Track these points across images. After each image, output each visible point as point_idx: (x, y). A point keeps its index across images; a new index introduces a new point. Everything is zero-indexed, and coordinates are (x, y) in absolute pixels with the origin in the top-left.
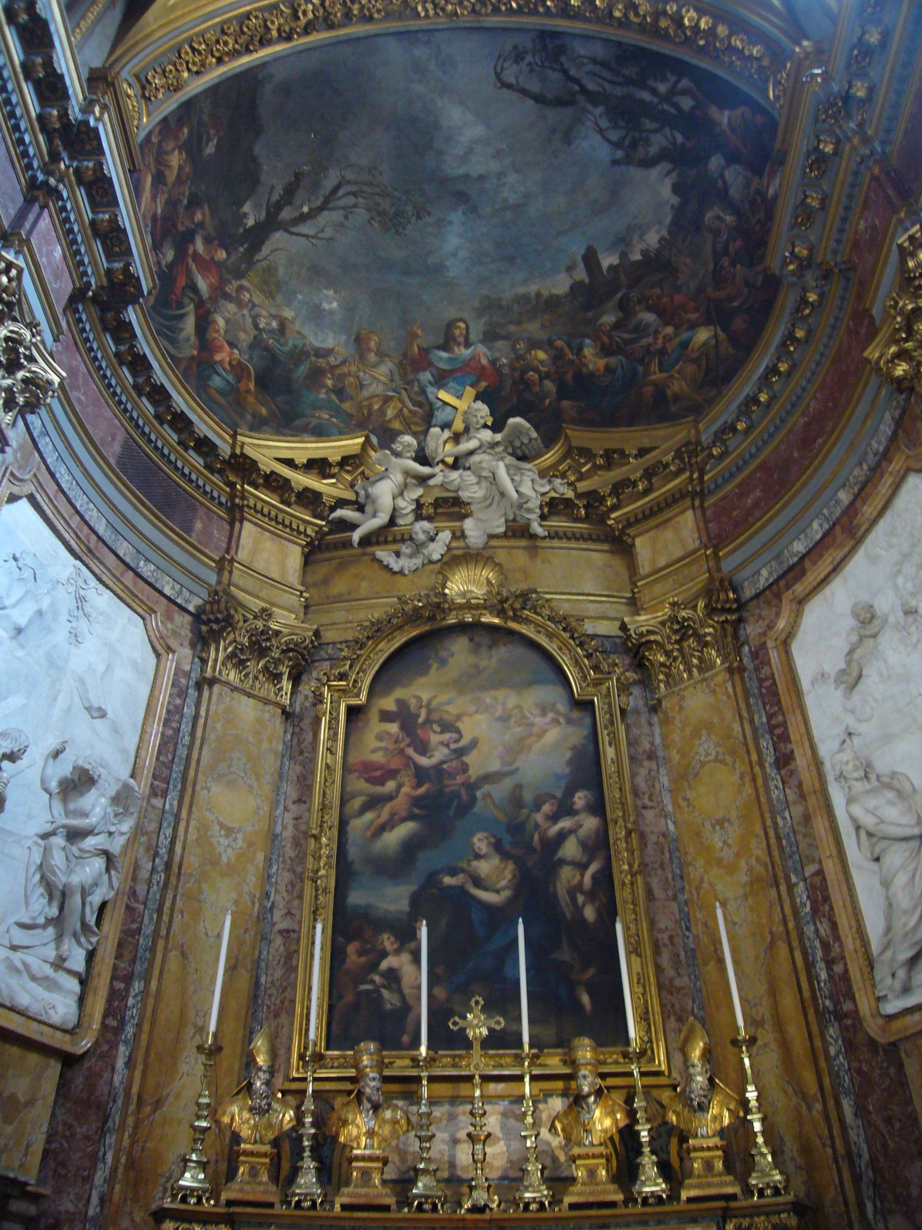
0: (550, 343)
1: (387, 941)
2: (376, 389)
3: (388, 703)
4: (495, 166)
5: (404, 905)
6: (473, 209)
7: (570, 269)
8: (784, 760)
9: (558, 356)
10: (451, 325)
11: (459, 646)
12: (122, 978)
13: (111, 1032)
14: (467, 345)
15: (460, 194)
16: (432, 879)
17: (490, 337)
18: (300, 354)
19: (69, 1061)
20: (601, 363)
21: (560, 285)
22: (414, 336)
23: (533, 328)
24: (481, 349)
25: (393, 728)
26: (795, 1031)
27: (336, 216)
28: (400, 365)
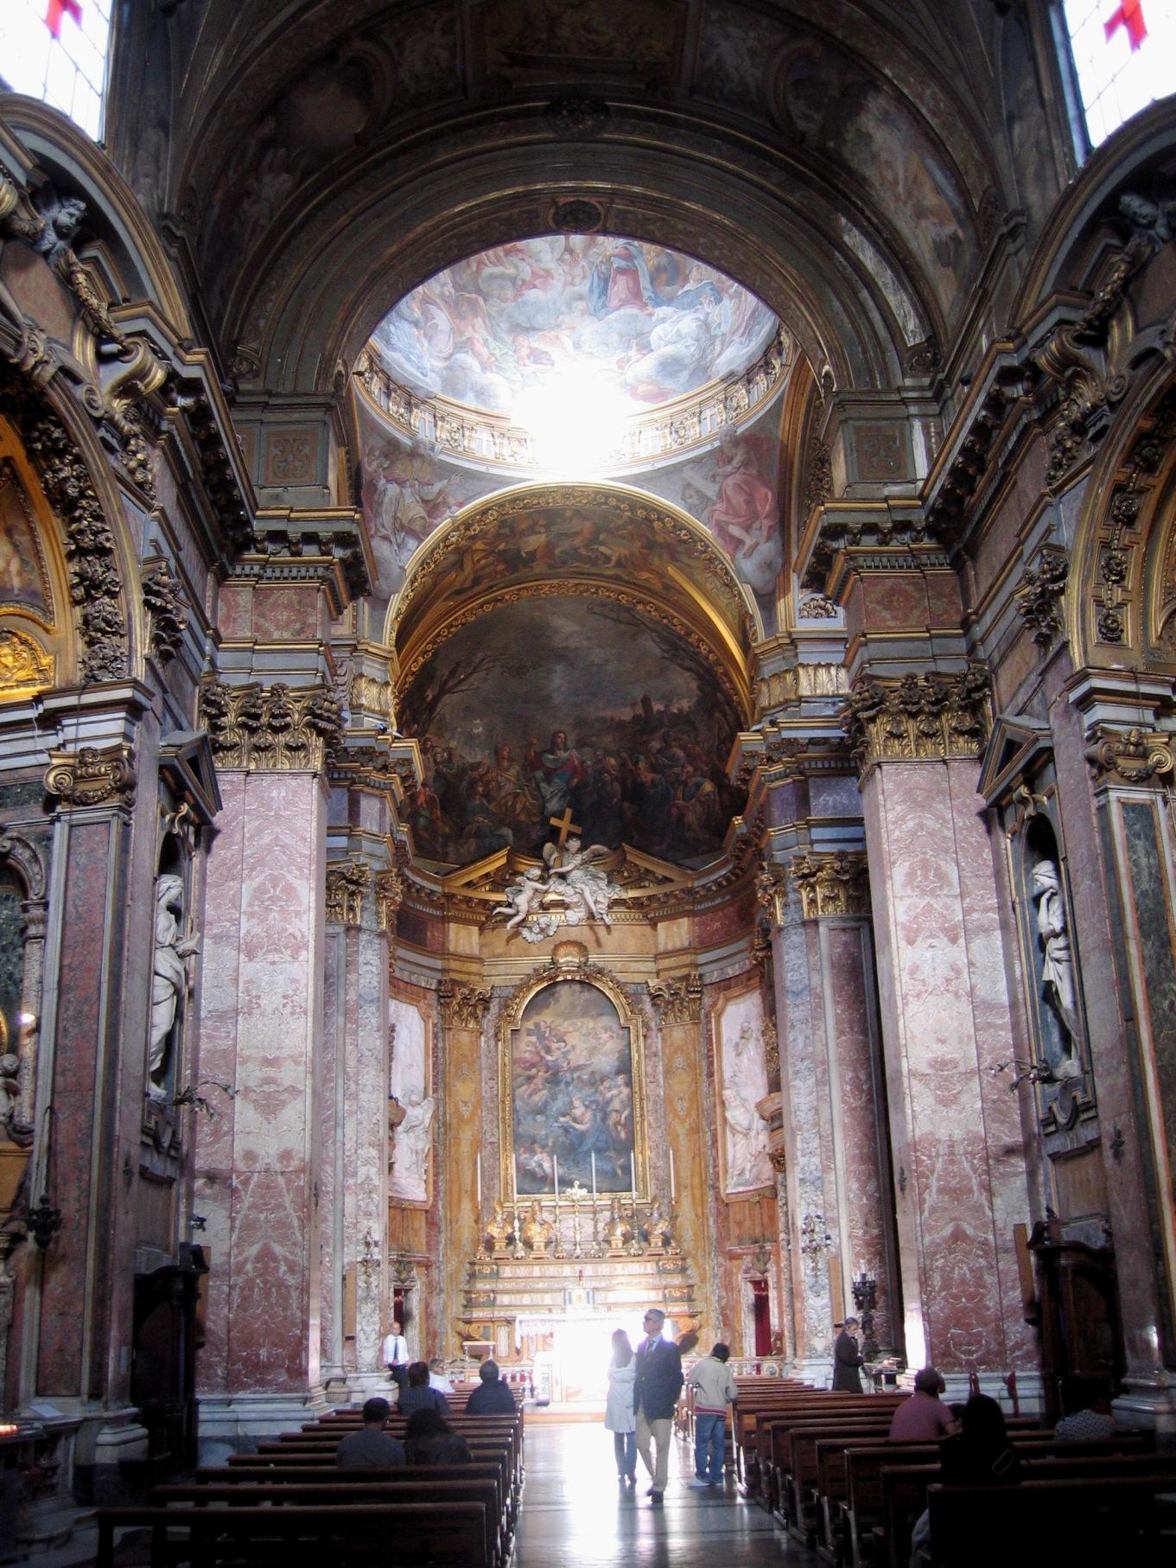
0: (618, 753)
2: (509, 788)
3: (530, 1025)
4: (585, 644)
6: (572, 664)
7: (633, 705)
8: (711, 1075)
9: (623, 764)
10: (555, 734)
11: (564, 991)
12: (436, 1175)
13: (435, 1200)
14: (566, 750)
15: (562, 656)
17: (581, 744)
18: (463, 770)
20: (651, 776)
21: (626, 714)
22: (531, 744)
23: (608, 740)
24: (575, 753)
25: (534, 1039)
26: (697, 1193)
27: (481, 674)
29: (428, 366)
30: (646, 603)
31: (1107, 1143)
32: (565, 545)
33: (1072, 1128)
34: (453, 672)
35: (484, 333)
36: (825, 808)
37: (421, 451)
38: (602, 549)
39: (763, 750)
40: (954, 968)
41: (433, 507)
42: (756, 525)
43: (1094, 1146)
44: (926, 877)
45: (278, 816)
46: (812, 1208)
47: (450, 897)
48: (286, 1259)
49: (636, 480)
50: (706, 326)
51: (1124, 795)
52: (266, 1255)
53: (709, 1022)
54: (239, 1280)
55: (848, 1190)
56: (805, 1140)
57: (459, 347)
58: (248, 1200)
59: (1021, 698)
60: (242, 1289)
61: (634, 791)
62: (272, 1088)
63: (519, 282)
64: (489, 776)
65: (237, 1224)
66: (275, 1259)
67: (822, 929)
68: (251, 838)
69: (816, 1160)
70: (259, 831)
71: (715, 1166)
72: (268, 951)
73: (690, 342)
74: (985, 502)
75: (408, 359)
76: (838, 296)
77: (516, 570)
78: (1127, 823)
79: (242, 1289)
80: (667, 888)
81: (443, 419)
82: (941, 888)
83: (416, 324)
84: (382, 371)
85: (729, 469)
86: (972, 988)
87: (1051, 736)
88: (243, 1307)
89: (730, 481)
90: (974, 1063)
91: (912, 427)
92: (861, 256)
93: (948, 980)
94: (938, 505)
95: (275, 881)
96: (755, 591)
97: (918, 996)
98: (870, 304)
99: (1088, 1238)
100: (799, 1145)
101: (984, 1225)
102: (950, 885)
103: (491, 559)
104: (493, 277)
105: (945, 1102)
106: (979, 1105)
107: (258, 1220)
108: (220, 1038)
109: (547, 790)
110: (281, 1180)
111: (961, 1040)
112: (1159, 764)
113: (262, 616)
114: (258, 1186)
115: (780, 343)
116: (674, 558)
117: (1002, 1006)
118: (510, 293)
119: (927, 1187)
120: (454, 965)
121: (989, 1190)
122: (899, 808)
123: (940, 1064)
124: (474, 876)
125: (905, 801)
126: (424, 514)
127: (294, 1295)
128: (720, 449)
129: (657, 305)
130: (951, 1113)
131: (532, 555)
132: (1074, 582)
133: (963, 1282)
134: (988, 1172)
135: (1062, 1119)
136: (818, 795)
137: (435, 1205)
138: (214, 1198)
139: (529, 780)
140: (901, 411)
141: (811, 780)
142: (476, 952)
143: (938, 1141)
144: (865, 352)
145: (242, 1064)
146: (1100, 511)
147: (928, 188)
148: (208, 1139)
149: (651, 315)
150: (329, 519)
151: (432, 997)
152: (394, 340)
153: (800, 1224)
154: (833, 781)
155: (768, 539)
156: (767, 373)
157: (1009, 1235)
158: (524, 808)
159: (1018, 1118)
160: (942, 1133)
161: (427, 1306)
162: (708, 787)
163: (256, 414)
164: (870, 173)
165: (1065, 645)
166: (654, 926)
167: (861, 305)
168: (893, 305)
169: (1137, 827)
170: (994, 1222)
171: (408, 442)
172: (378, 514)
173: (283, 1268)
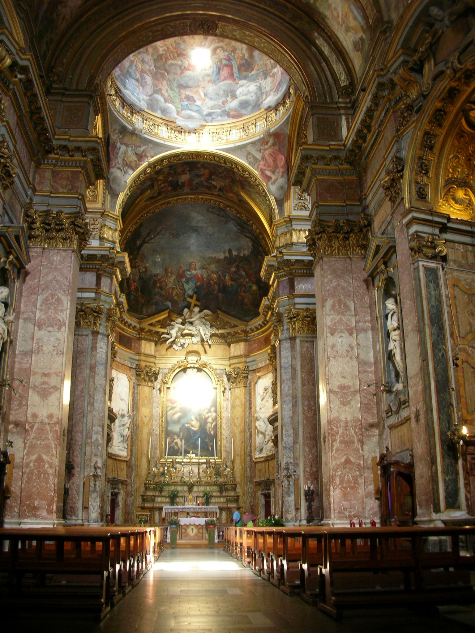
1: (175, 437)
4: (206, 225)
5: (178, 430)
7: (224, 252)
8: (250, 408)
9: (219, 277)
10: (191, 264)
12: (132, 446)
13: (131, 456)
14: (195, 270)
16: (184, 425)
17: (202, 268)
18: (151, 277)
19: (127, 461)
21: (221, 256)
22: (181, 267)
24: (199, 271)
26: (243, 457)
27: (161, 236)
28: (177, 277)
29: (141, 98)
30: (230, 207)
31: (413, 416)
32: (197, 180)
33: (398, 413)
34: (148, 234)
35: (167, 87)
36: (301, 290)
37: (136, 132)
38: (213, 182)
39: (275, 264)
40: (351, 346)
41: (140, 157)
42: (277, 171)
43: (408, 419)
44: (340, 307)
45: (56, 268)
46: (288, 459)
47: (142, 330)
48: (48, 462)
49: (227, 150)
50: (260, 88)
51: (425, 264)
52: (40, 460)
53: (250, 386)
54: (27, 470)
55: (304, 451)
56: (287, 430)
57: (155, 92)
58: (33, 435)
59: (383, 228)
60: (28, 474)
61: (224, 289)
62: (46, 386)
63: (183, 68)
64: (162, 280)
65: (27, 445)
66: (43, 461)
67: (298, 341)
68: (44, 277)
69: (291, 439)
70: (47, 274)
71: (251, 447)
72: (48, 327)
73: (253, 94)
74: (370, 146)
75: (133, 94)
76: (313, 64)
77: (177, 190)
78: (426, 276)
79: (28, 474)
80: (235, 329)
81: (146, 120)
82: (346, 312)
83: (137, 80)
84: (121, 97)
85: (266, 147)
86: (358, 355)
87: (395, 241)
88: (28, 482)
89: (267, 152)
90: (358, 387)
91: (341, 118)
92: (323, 49)
93: (348, 351)
94: (351, 148)
95: (53, 296)
96: (275, 199)
97: (335, 358)
98: (326, 68)
99: (403, 459)
100: (284, 433)
101: (359, 457)
102: (350, 311)
103: (166, 184)
104: (172, 65)
105: (345, 403)
106: (359, 405)
107: (37, 444)
108: (24, 363)
109: (186, 287)
110: (48, 427)
111: (352, 377)
112: (441, 251)
113: (55, 182)
114: (38, 429)
115: (290, 93)
116: (243, 188)
117: (371, 363)
118: (179, 71)
119: (335, 440)
120: (143, 358)
121: (362, 442)
122: (329, 277)
123: (343, 387)
124: (154, 321)
125: (332, 274)
126: (136, 159)
127: (51, 478)
128: (263, 138)
129: (240, 79)
130: (347, 409)
131: (183, 184)
132: (407, 172)
133: (349, 481)
134: (361, 435)
135: (394, 409)
136: (298, 284)
137: (131, 459)
138: (18, 433)
139: (179, 282)
140: (337, 112)
141: (295, 278)
142: (153, 353)
143: (341, 420)
144: (323, 87)
145: (33, 375)
146: (419, 142)
147: (351, 19)
148: (16, 407)
149: (237, 83)
150: (87, 141)
151: (133, 371)
152: (128, 86)
153: (283, 465)
154: (305, 278)
155: (282, 177)
156: (284, 106)
157: (370, 462)
158: (177, 294)
159: (375, 412)
160: (343, 417)
161: (126, 501)
162: (254, 287)
163: (59, 98)
164: (327, 13)
165: (403, 199)
166: (229, 346)
167: (322, 69)
168: (335, 70)
169: (431, 278)
170: (363, 456)
171: (131, 128)
172: (116, 158)
173: (47, 466)
